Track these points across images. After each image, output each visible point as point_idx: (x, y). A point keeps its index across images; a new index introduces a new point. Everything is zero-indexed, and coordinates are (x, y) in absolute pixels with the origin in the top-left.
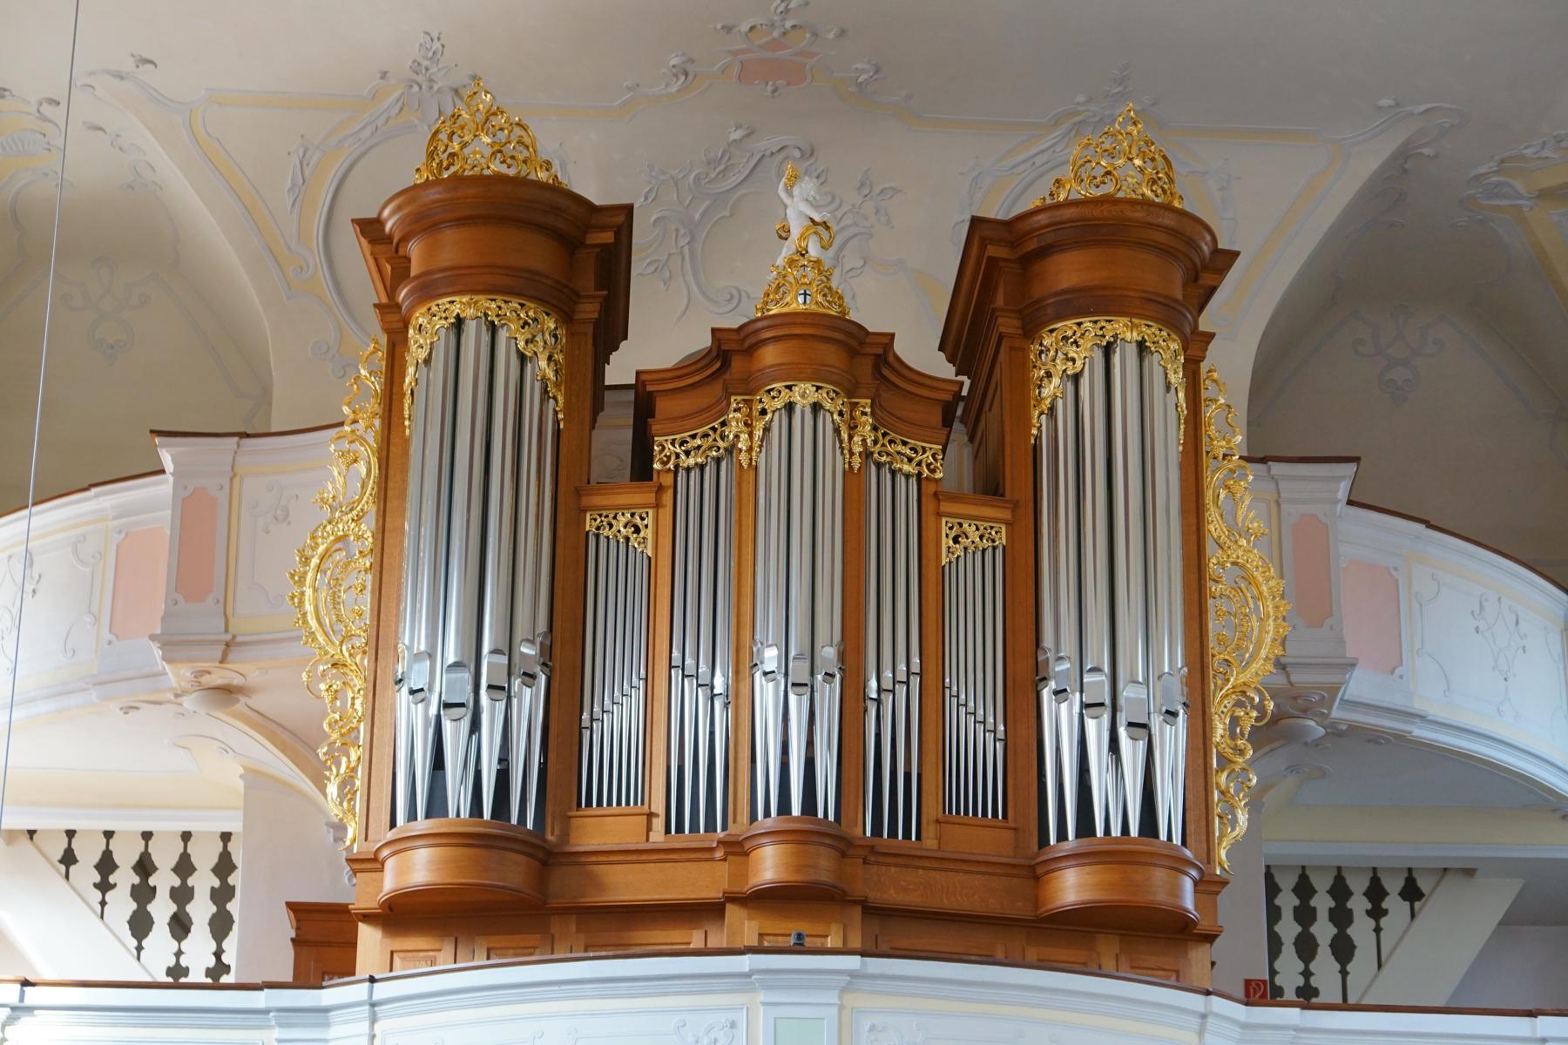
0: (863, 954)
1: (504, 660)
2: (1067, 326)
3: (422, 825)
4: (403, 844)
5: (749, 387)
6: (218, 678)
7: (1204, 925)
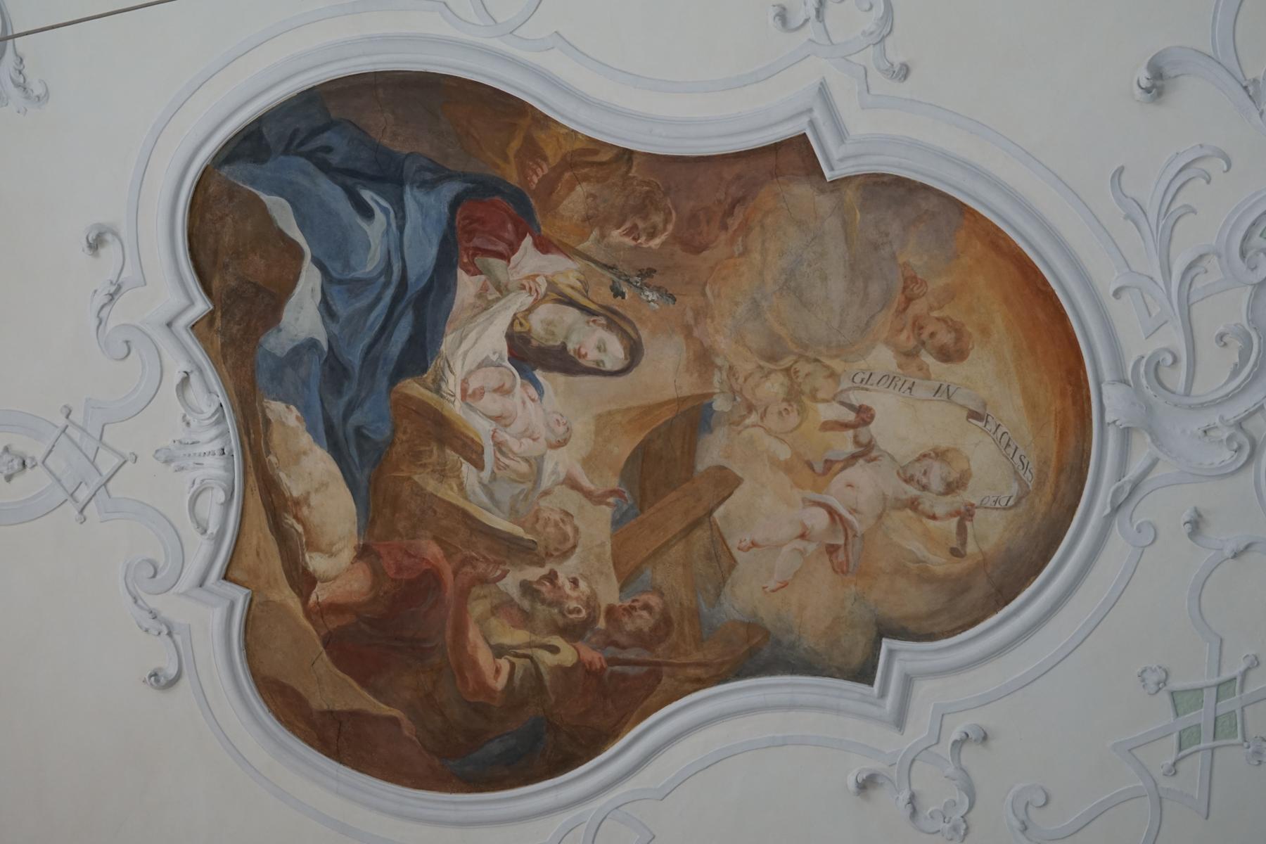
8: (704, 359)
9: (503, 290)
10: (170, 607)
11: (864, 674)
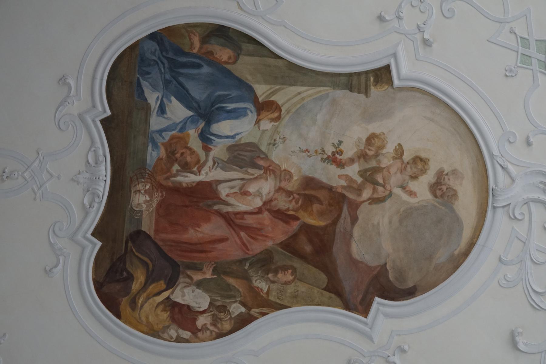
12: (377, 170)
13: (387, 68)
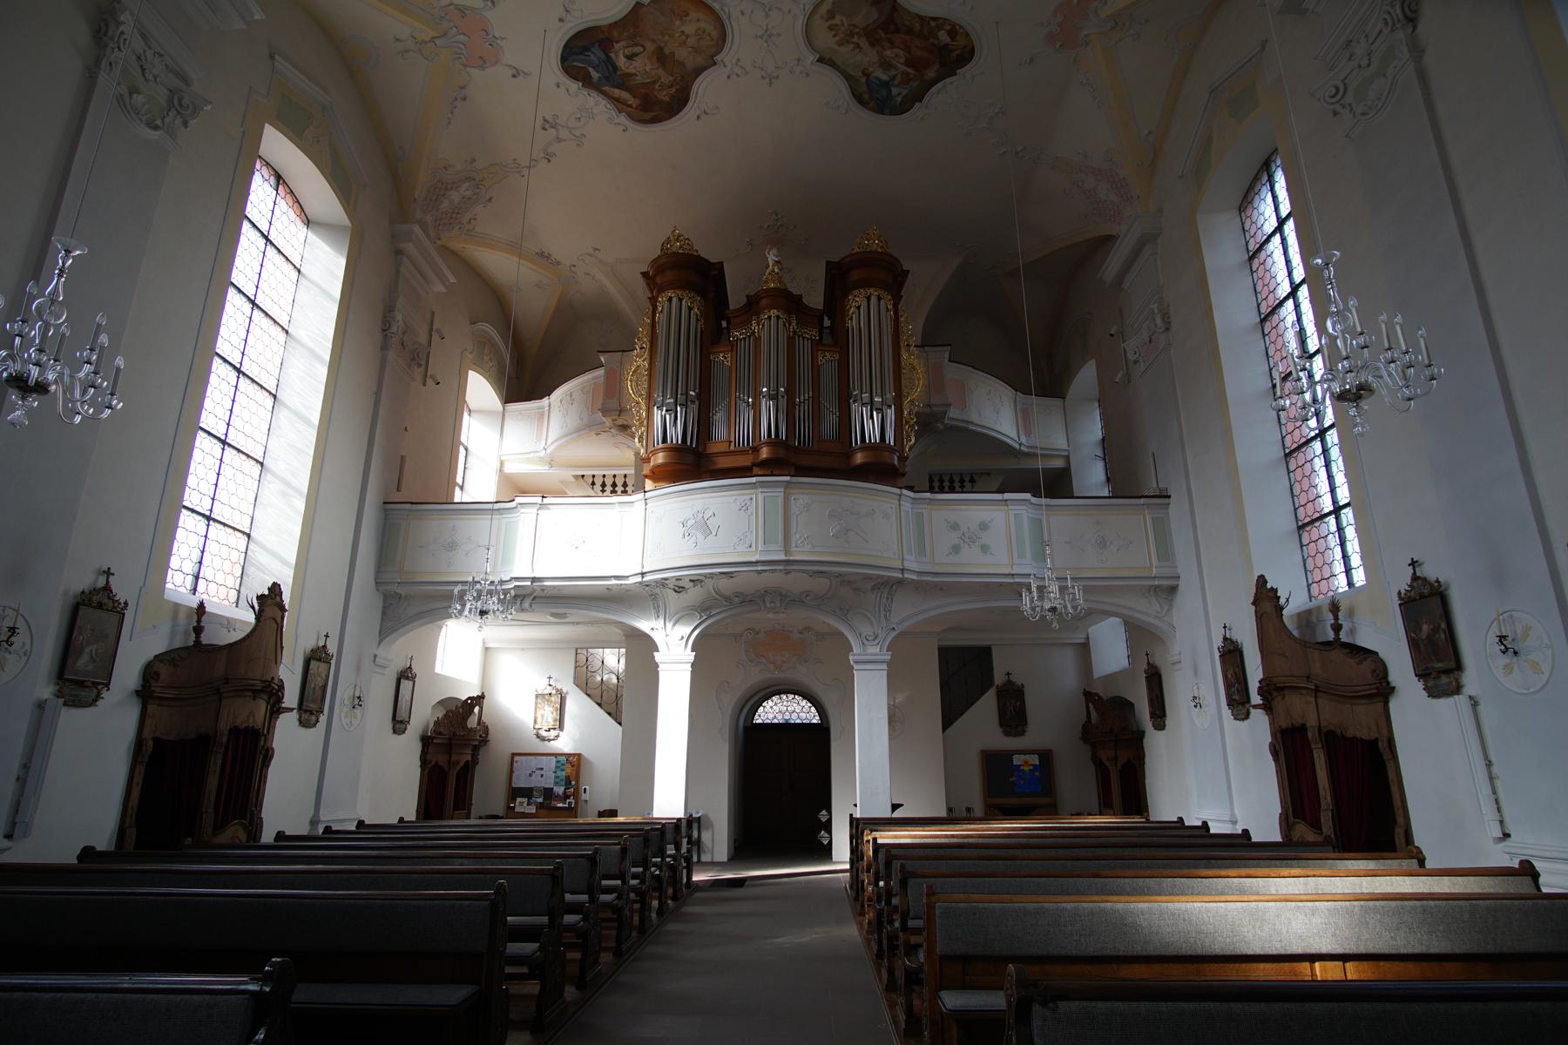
0: (791, 476)
1: (685, 397)
2: (856, 292)
3: (661, 445)
4: (655, 452)
5: (758, 314)
6: (620, 422)
7: (901, 470)
8: (654, 41)
9: (618, 52)
10: (616, 121)
11: (715, 64)
12: (847, 35)
13: (818, 61)
